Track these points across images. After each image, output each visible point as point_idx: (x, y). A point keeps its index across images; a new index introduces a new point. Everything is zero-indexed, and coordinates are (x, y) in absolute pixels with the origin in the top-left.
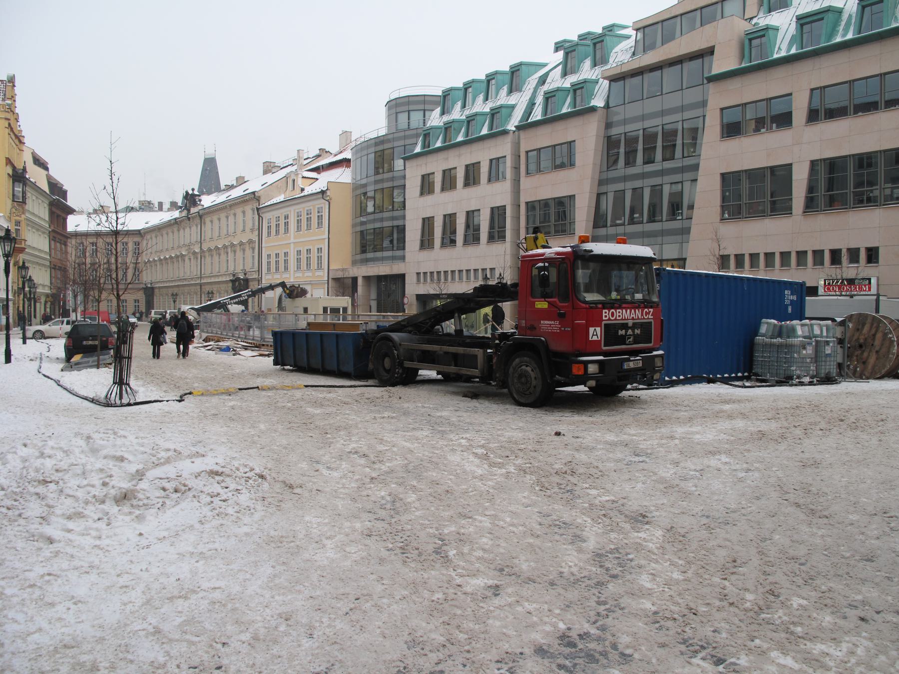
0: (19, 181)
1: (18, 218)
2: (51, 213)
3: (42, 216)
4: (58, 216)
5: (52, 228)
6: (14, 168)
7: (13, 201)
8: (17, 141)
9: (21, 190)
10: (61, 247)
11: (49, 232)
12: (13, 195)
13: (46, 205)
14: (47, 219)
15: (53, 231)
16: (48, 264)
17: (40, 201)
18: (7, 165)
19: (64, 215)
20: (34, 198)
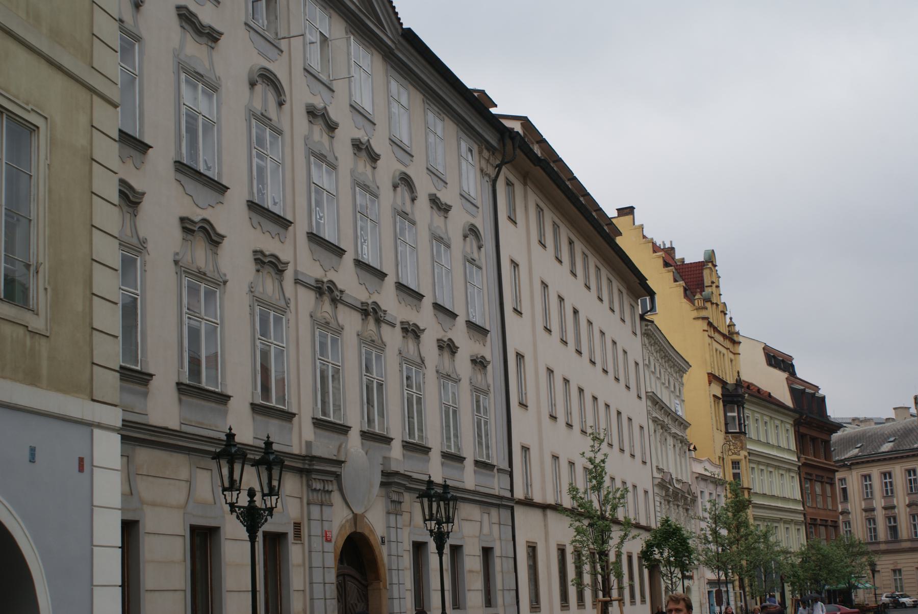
0: (732, 402)
1: (735, 457)
2: (801, 438)
3: (784, 444)
4: (814, 439)
5: (803, 460)
6: (723, 384)
7: (727, 432)
8: (728, 344)
9: (735, 414)
10: (823, 490)
11: (799, 468)
12: (726, 424)
13: (788, 426)
14: (793, 447)
15: (804, 464)
16: (801, 518)
17: (778, 423)
18: (710, 383)
19: (824, 437)
20: (767, 419)
